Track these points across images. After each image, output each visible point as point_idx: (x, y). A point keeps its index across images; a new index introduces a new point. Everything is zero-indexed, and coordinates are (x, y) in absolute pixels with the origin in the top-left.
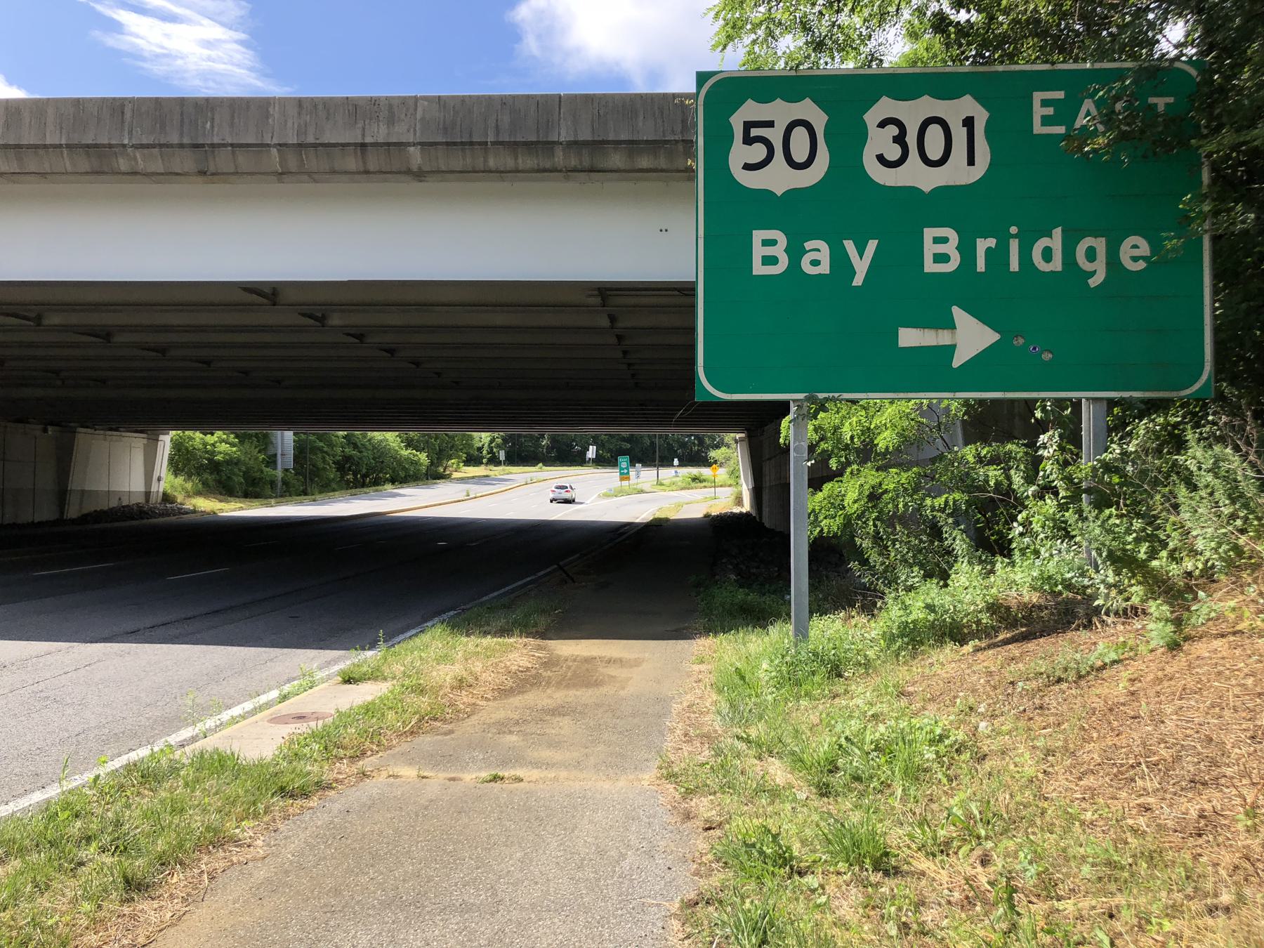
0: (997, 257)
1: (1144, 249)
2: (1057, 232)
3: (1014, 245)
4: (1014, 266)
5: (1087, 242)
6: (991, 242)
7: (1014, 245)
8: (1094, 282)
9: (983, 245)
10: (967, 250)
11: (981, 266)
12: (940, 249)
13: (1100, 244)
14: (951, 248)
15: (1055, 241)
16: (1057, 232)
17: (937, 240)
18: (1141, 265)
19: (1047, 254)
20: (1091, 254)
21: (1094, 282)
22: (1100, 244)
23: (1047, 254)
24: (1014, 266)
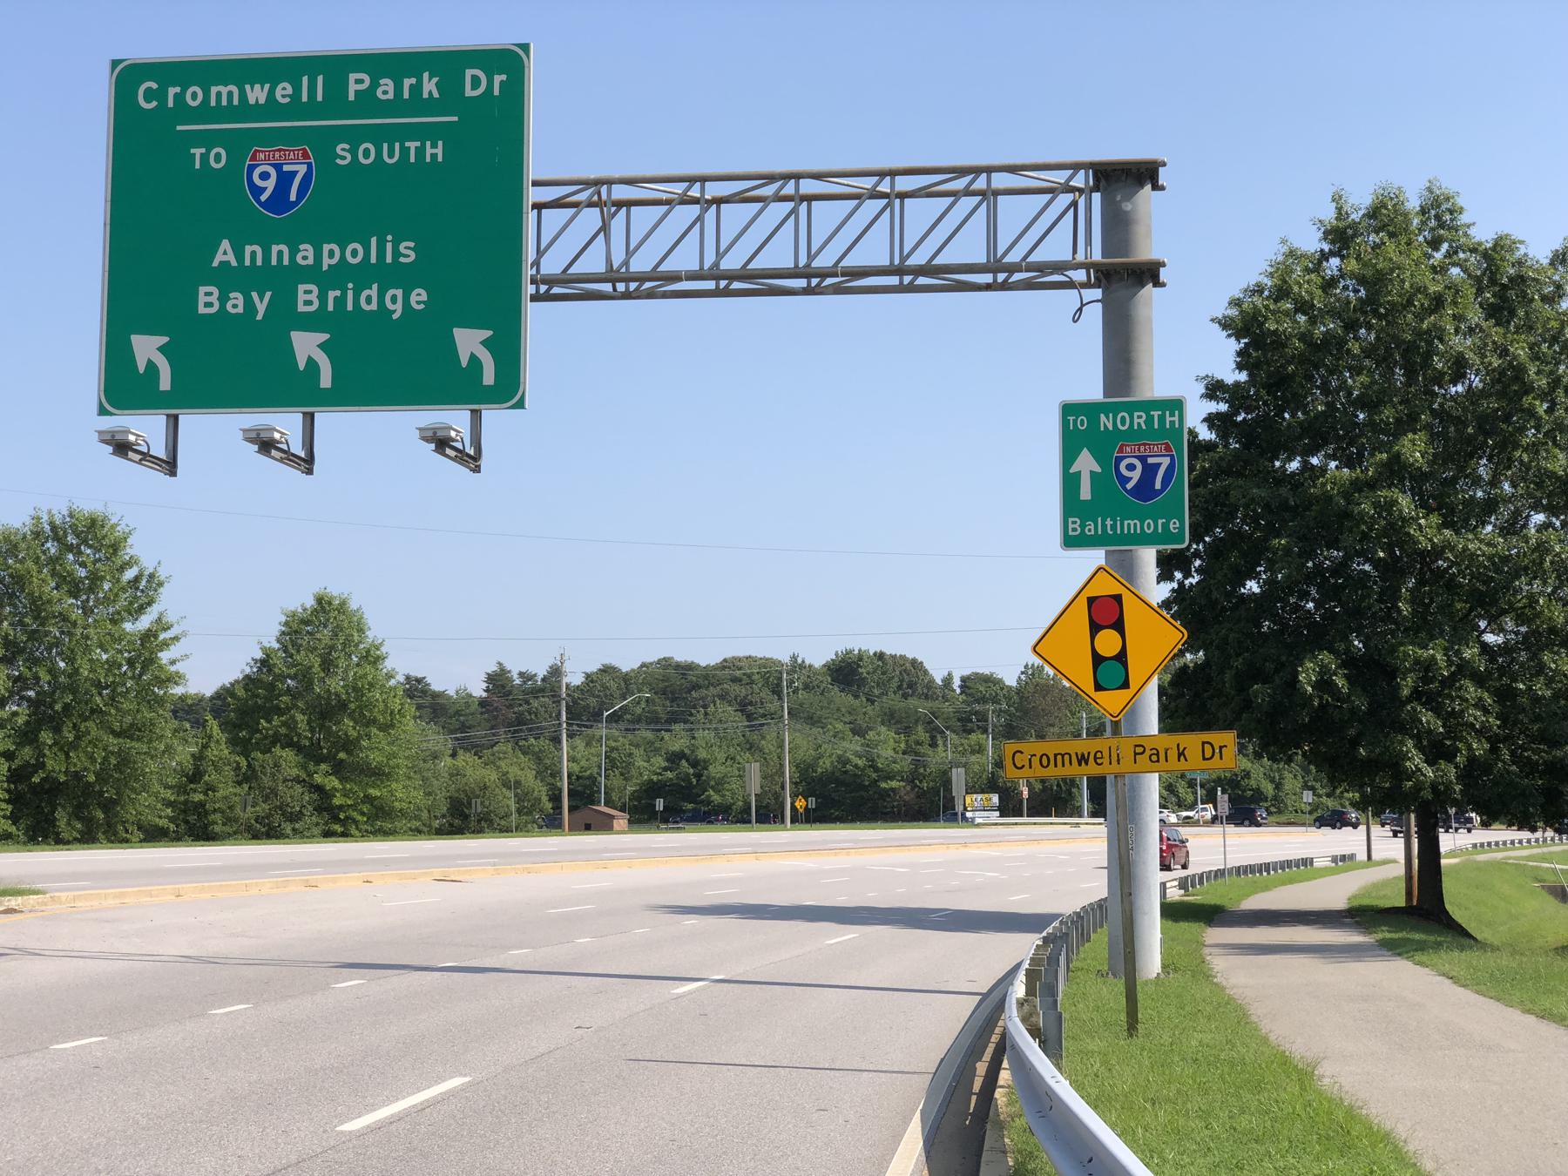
0: (340, 302)
1: (424, 297)
2: (375, 286)
3: (350, 294)
4: (350, 307)
5: (391, 292)
6: (338, 293)
7: (350, 294)
8: (395, 316)
9: (332, 294)
10: (323, 298)
11: (330, 308)
12: (307, 297)
13: (399, 293)
14: (313, 297)
15: (373, 291)
16: (375, 286)
17: (306, 292)
18: (422, 306)
19: (369, 300)
20: (394, 299)
21: (395, 316)
22: (399, 293)
23: (369, 300)
24: (350, 307)
